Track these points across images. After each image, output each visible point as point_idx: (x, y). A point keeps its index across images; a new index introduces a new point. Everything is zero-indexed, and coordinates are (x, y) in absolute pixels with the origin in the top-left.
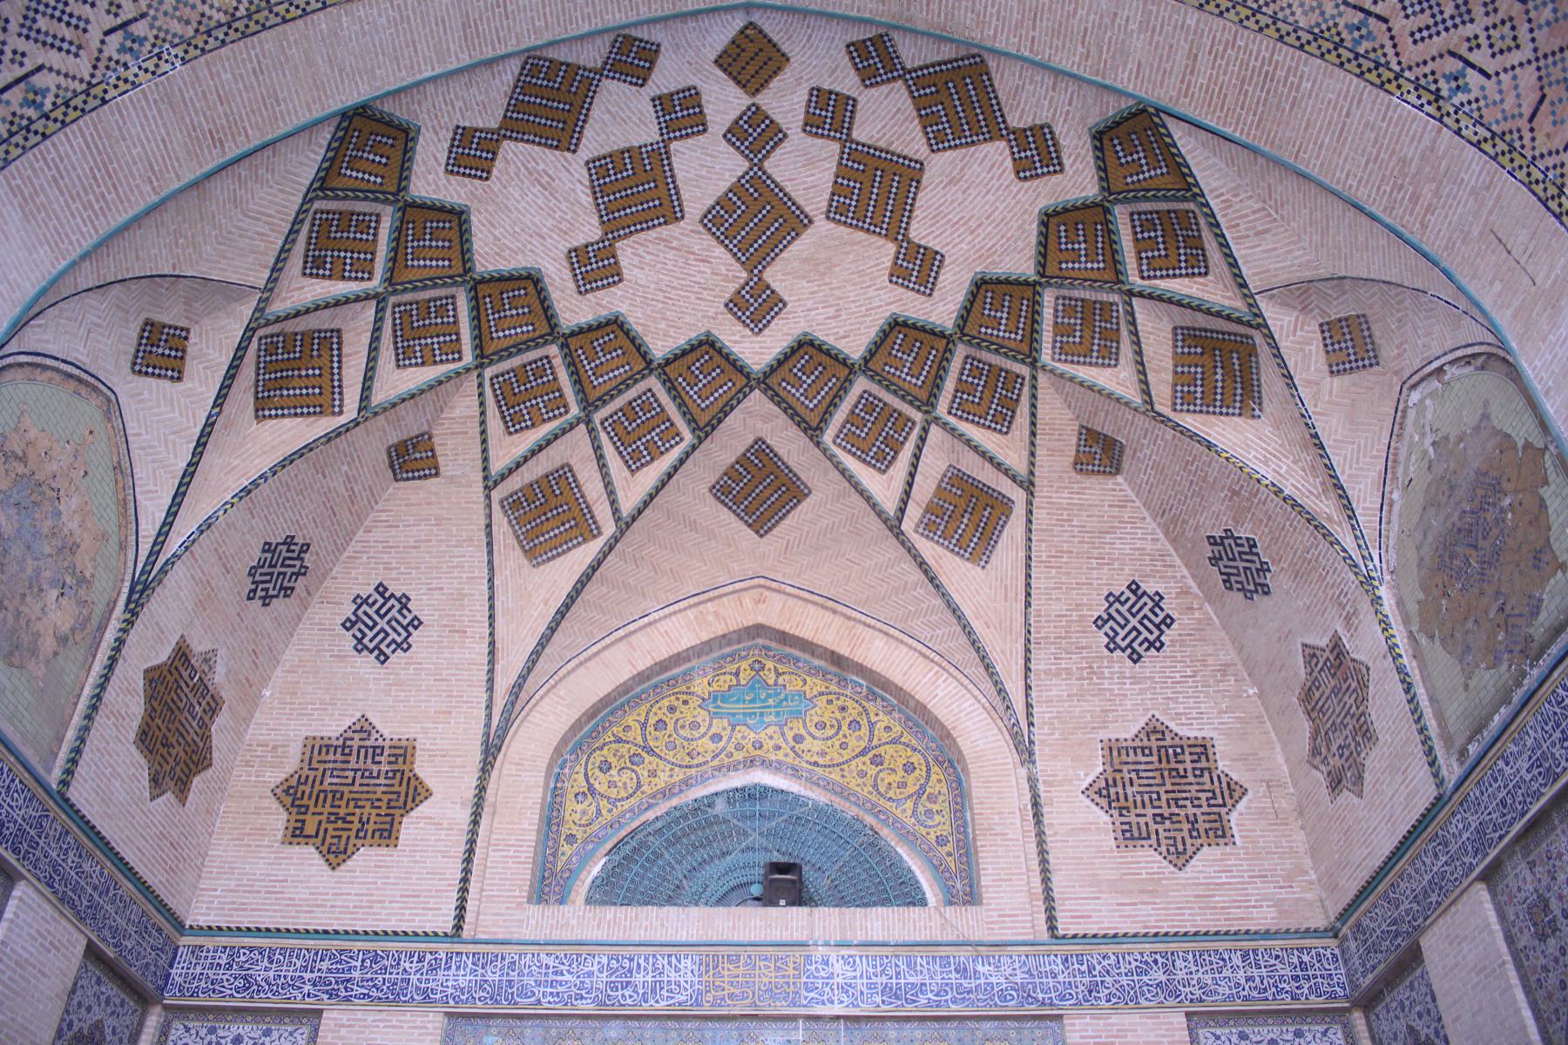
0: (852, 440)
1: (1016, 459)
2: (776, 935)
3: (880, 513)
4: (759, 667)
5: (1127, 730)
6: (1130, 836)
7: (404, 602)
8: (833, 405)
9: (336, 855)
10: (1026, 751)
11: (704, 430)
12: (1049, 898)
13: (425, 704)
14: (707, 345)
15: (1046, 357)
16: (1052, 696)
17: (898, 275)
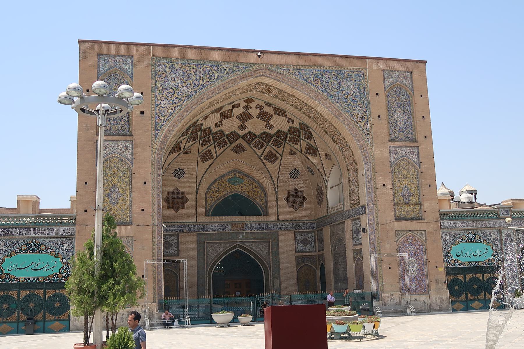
0: (255, 145)
1: (281, 152)
2: (241, 220)
3: (258, 156)
4: (235, 174)
5: (291, 189)
6: (290, 206)
7: (183, 170)
8: (253, 141)
9: (176, 210)
10: (276, 193)
11: (231, 143)
12: (278, 215)
13: (186, 185)
14: (234, 132)
15: (287, 141)
16: (281, 184)
17: (266, 126)
